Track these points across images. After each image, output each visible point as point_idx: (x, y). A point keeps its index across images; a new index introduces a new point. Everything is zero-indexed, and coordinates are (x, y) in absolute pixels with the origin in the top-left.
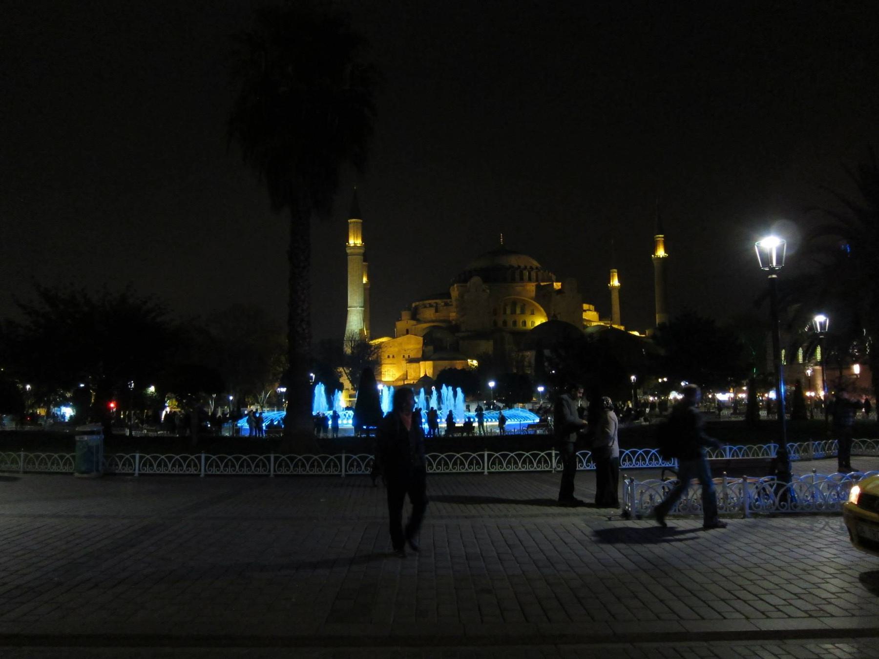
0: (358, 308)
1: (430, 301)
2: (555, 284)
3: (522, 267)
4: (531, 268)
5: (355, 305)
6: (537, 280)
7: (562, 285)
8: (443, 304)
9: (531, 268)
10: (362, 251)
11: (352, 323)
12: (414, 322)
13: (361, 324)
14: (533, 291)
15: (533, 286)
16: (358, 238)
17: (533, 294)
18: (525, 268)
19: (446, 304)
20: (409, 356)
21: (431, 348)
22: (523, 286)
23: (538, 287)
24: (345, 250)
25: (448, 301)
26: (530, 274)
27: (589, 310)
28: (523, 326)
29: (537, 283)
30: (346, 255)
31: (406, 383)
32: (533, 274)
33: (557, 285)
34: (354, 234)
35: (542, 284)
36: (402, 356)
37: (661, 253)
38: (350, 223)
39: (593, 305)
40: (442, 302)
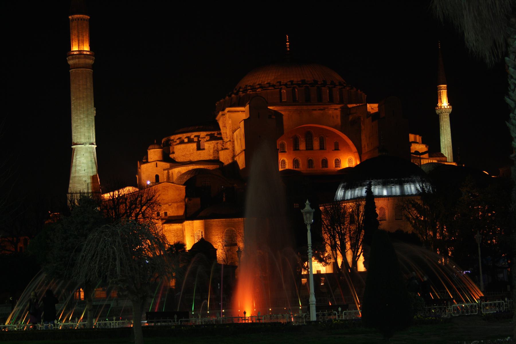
0: (88, 146)
1: (189, 135)
2: (368, 105)
3: (319, 83)
5: (83, 140)
6: (341, 102)
7: (378, 107)
8: (208, 138)
10: (91, 62)
11: (78, 168)
12: (167, 165)
13: (92, 168)
14: (337, 116)
15: (335, 109)
16: (84, 42)
17: (339, 121)
19: (212, 138)
21: (198, 200)
22: (324, 109)
23: (345, 112)
25: (216, 133)
27: (415, 142)
28: (323, 167)
30: (68, 67)
33: (370, 106)
34: (78, 37)
35: (350, 106)
38: (73, 20)
39: (420, 136)
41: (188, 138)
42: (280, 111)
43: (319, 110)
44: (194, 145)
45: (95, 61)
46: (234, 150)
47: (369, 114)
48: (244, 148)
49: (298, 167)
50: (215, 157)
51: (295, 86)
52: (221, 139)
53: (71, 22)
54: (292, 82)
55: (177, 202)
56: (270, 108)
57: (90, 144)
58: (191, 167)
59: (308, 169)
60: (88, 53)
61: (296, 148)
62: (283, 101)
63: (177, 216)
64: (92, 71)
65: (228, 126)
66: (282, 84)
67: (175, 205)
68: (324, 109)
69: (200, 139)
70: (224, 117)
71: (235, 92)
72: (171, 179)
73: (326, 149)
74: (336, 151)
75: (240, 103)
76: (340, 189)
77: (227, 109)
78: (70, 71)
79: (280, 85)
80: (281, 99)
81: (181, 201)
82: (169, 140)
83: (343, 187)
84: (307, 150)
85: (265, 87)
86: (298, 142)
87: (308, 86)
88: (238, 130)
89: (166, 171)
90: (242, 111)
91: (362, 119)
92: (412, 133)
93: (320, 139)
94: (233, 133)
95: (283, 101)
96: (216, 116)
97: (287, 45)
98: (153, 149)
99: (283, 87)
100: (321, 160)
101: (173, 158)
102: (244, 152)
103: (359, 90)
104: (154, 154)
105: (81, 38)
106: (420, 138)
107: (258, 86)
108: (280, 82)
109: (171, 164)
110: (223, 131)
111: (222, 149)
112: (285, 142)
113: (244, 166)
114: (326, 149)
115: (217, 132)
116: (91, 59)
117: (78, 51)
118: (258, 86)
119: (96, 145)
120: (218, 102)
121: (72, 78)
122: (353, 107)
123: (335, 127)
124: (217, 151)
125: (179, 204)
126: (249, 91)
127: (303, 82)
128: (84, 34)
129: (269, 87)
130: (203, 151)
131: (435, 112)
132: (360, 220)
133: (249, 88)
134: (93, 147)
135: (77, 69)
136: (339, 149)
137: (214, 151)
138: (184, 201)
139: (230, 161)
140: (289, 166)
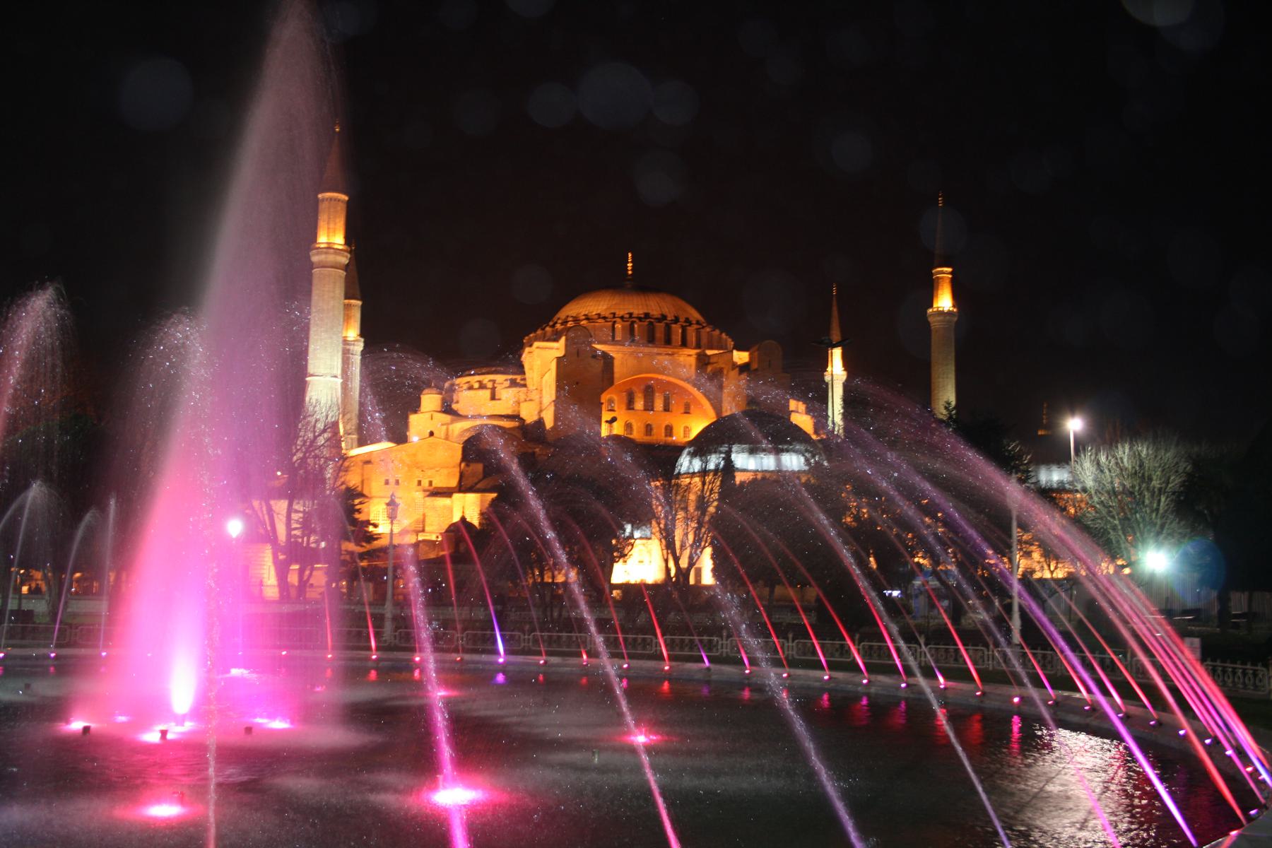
0: (328, 378)
3: (669, 319)
5: (322, 371)
6: (698, 346)
7: (750, 355)
8: (508, 383)
10: (344, 260)
12: (447, 418)
14: (691, 366)
15: (690, 355)
18: (676, 320)
19: (514, 384)
20: (431, 483)
21: (479, 467)
22: (672, 354)
23: (703, 361)
24: (309, 257)
25: (518, 378)
26: (684, 329)
28: (666, 436)
29: (698, 351)
30: (311, 266)
31: (420, 538)
34: (328, 223)
35: (709, 352)
36: (416, 483)
37: (944, 301)
38: (323, 200)
40: (506, 380)
41: (480, 382)
42: (609, 352)
43: (667, 354)
44: (487, 393)
45: (350, 259)
46: (541, 403)
47: (734, 365)
48: (554, 398)
49: (631, 434)
50: (514, 411)
52: (525, 386)
53: (320, 203)
54: (631, 314)
55: (447, 467)
56: (598, 346)
58: (478, 422)
60: (341, 247)
61: (630, 405)
63: (448, 488)
64: (345, 273)
66: (616, 316)
67: (445, 471)
69: (496, 385)
70: (531, 355)
71: (551, 323)
72: (450, 438)
73: (671, 411)
74: (685, 415)
76: (684, 456)
77: (536, 344)
79: (614, 317)
80: (613, 337)
81: (454, 467)
82: (453, 385)
83: (689, 453)
85: (592, 319)
86: (633, 398)
87: (652, 320)
89: (445, 427)
93: (665, 397)
95: (616, 339)
96: (520, 356)
97: (628, 267)
99: (618, 320)
100: (664, 426)
101: (456, 409)
102: (553, 404)
104: (430, 400)
105: (332, 226)
107: (584, 317)
108: (614, 314)
109: (455, 418)
110: (528, 374)
111: (526, 401)
112: (615, 397)
114: (671, 411)
116: (343, 256)
117: (328, 243)
119: (342, 378)
120: (527, 338)
121: (315, 281)
123: (687, 380)
124: (518, 403)
126: (570, 323)
127: (647, 315)
128: (338, 220)
129: (599, 318)
130: (498, 402)
132: (705, 490)
133: (571, 319)
134: (336, 383)
136: (691, 411)
139: (536, 418)
140: (618, 429)
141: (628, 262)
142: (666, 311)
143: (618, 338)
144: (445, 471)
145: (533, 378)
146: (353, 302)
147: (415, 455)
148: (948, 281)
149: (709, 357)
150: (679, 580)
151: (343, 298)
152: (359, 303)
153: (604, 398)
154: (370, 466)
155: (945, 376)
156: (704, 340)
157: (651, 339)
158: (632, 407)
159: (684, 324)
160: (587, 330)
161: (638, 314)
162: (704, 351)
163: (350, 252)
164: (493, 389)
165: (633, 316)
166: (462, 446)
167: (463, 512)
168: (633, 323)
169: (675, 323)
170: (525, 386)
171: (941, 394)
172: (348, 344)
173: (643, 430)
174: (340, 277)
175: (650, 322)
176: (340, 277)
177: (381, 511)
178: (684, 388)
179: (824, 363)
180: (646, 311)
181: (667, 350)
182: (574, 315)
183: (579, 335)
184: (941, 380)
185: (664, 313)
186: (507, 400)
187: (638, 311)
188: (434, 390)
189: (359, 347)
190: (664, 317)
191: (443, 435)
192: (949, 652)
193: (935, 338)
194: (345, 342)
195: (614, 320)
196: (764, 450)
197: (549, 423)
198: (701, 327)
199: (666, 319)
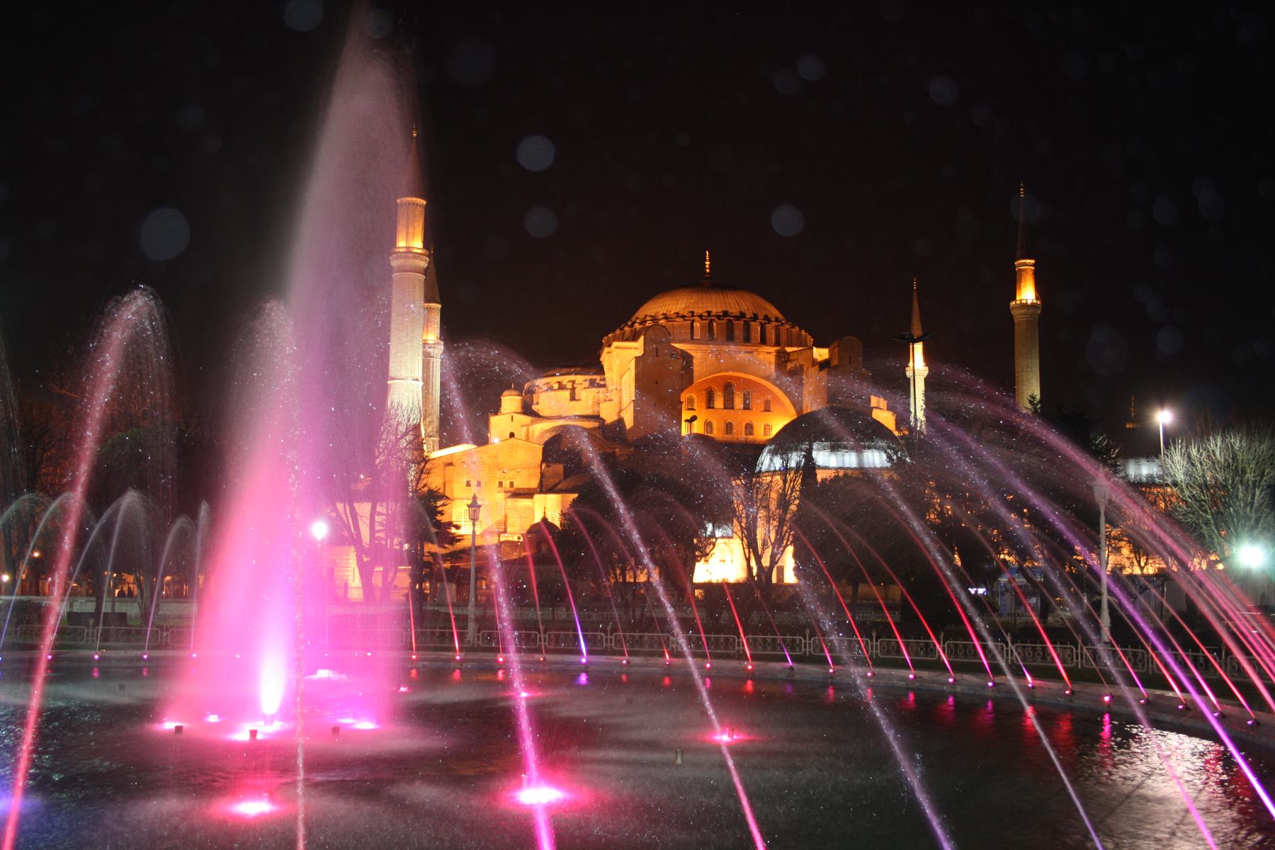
0: (410, 381)
3: (748, 316)
4: (764, 319)
5: (403, 374)
6: (777, 343)
7: (829, 351)
8: (587, 384)
9: (764, 319)
10: (423, 264)
12: (527, 419)
14: (770, 363)
18: (755, 318)
19: (592, 384)
20: (512, 484)
21: (560, 468)
25: (598, 378)
30: (391, 270)
31: (503, 539)
32: (770, 328)
35: (789, 349)
36: (497, 484)
37: (1027, 293)
38: (402, 205)
40: (586, 380)
41: (559, 383)
42: (688, 351)
44: (567, 394)
45: (429, 264)
47: (814, 362)
49: (711, 433)
51: (713, 318)
53: (399, 208)
54: (709, 313)
55: (529, 468)
56: (677, 345)
57: (413, 380)
58: (560, 423)
59: (725, 436)
60: (420, 251)
61: (710, 404)
62: (695, 338)
63: (529, 489)
65: (615, 368)
66: (695, 314)
67: (526, 472)
68: (752, 352)
69: (575, 386)
70: (610, 355)
71: (629, 323)
72: (531, 439)
74: (767, 413)
75: (634, 338)
77: (615, 344)
78: (393, 275)
79: (693, 316)
81: (535, 468)
83: (769, 452)
84: (725, 408)
86: (713, 397)
87: (731, 318)
88: (628, 372)
89: (525, 428)
90: (635, 348)
91: (805, 370)
92: (875, 395)
94: (621, 378)
95: (695, 338)
96: (600, 356)
98: (508, 395)
99: (697, 318)
100: (744, 425)
101: (536, 410)
102: (632, 404)
103: (803, 331)
104: (510, 402)
105: (411, 230)
106: (886, 402)
107: (662, 316)
108: (693, 312)
109: (533, 418)
112: (695, 397)
113: (632, 424)
115: (599, 376)
117: (407, 248)
118: (662, 316)
120: (605, 338)
122: (793, 352)
123: (767, 378)
125: (531, 471)
127: (725, 313)
128: (416, 225)
130: (579, 402)
131: (905, 374)
132: (787, 488)
133: (649, 318)
135: (402, 273)
137: (593, 403)
138: (539, 468)
139: (615, 418)
140: (698, 428)
141: (706, 260)
142: (744, 309)
143: (697, 336)
144: (526, 472)
145: (612, 379)
146: (433, 305)
147: (496, 457)
148: (1031, 273)
149: (789, 354)
150: (761, 578)
151: (423, 302)
152: (439, 306)
153: (684, 396)
154: (451, 468)
155: (1029, 369)
156: (783, 337)
157: (730, 338)
158: (712, 405)
159: (763, 322)
160: (666, 329)
161: (717, 312)
162: (784, 348)
163: (429, 257)
164: (573, 389)
165: (712, 314)
166: (542, 447)
167: (545, 513)
168: (711, 321)
169: (754, 321)
170: (604, 386)
171: (1025, 388)
172: (430, 347)
173: (723, 427)
174: (419, 280)
175: (729, 320)
176: (419, 280)
177: (463, 512)
178: (764, 386)
179: (905, 356)
180: (725, 309)
181: (746, 347)
182: (653, 314)
183: (657, 336)
184: (1025, 374)
185: (743, 311)
186: (587, 399)
187: (716, 309)
188: (513, 392)
189: (438, 350)
190: (743, 315)
191: (523, 437)
192: (1036, 650)
193: (1018, 331)
194: (425, 344)
195: (692, 319)
196: (845, 447)
197: (629, 423)
198: (780, 324)
199: (745, 317)
